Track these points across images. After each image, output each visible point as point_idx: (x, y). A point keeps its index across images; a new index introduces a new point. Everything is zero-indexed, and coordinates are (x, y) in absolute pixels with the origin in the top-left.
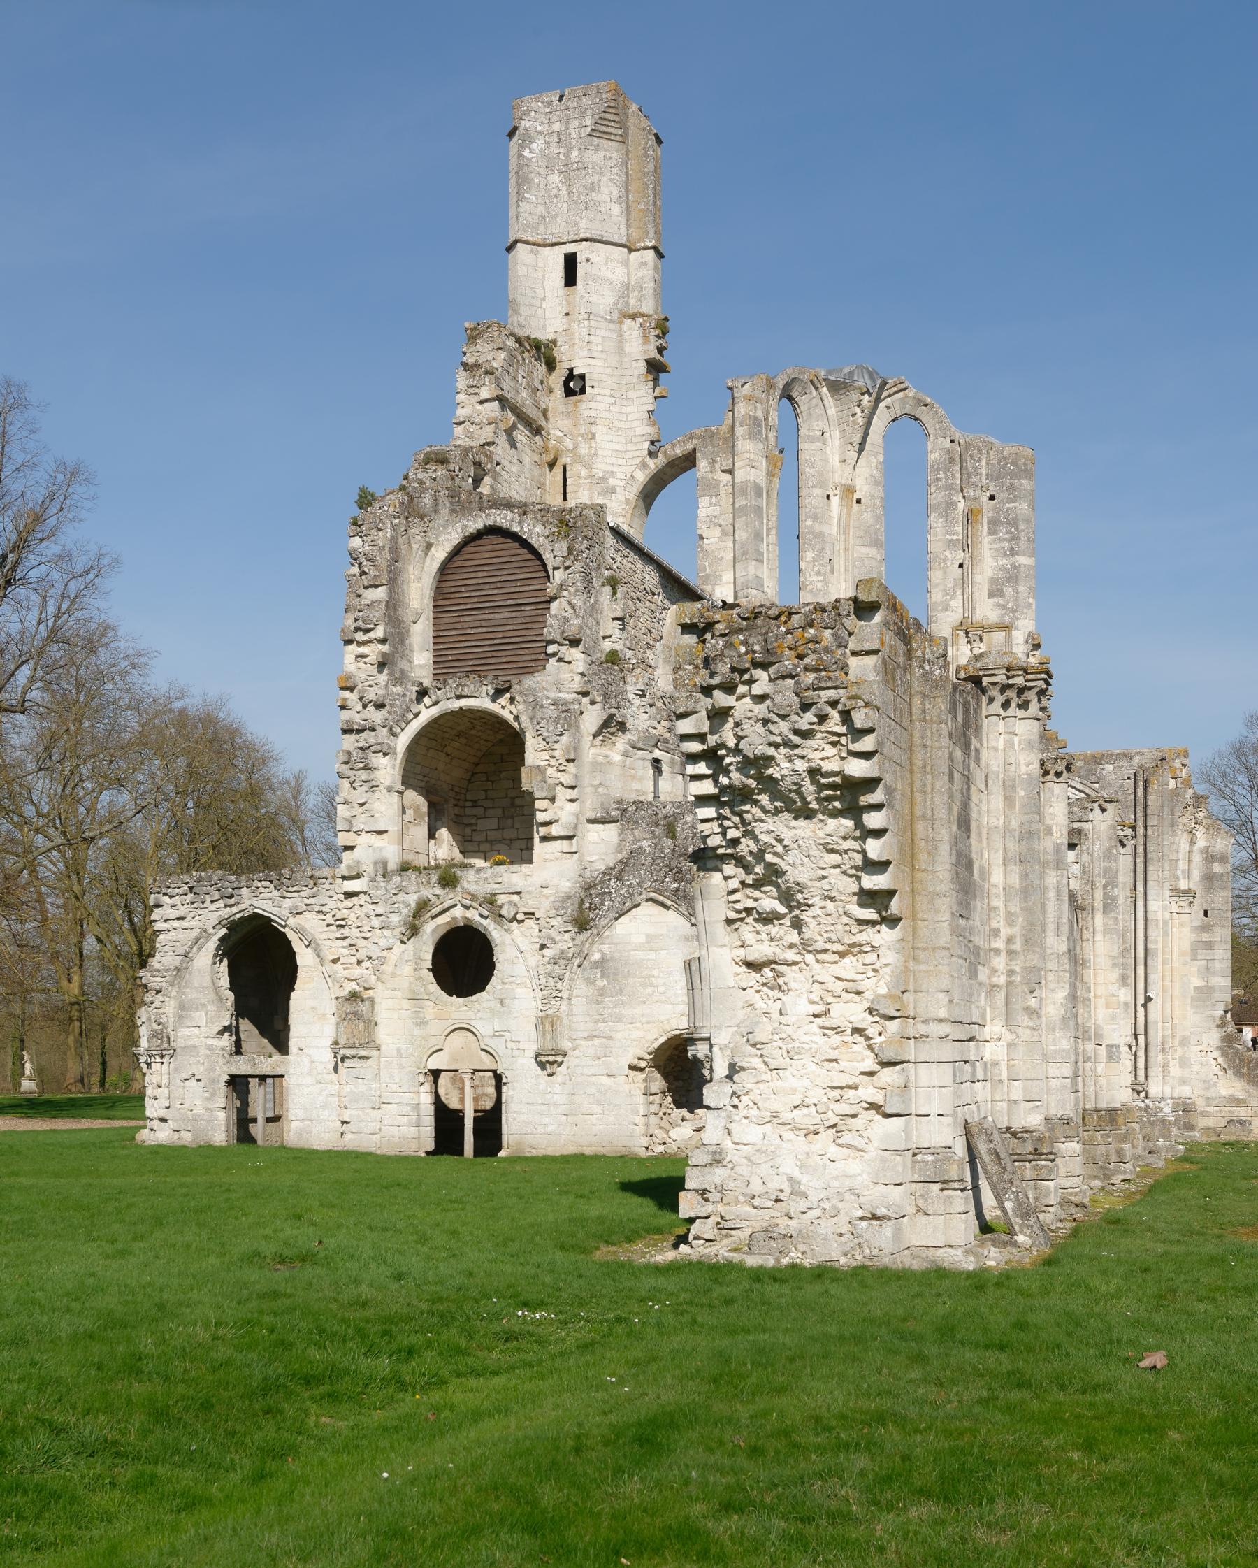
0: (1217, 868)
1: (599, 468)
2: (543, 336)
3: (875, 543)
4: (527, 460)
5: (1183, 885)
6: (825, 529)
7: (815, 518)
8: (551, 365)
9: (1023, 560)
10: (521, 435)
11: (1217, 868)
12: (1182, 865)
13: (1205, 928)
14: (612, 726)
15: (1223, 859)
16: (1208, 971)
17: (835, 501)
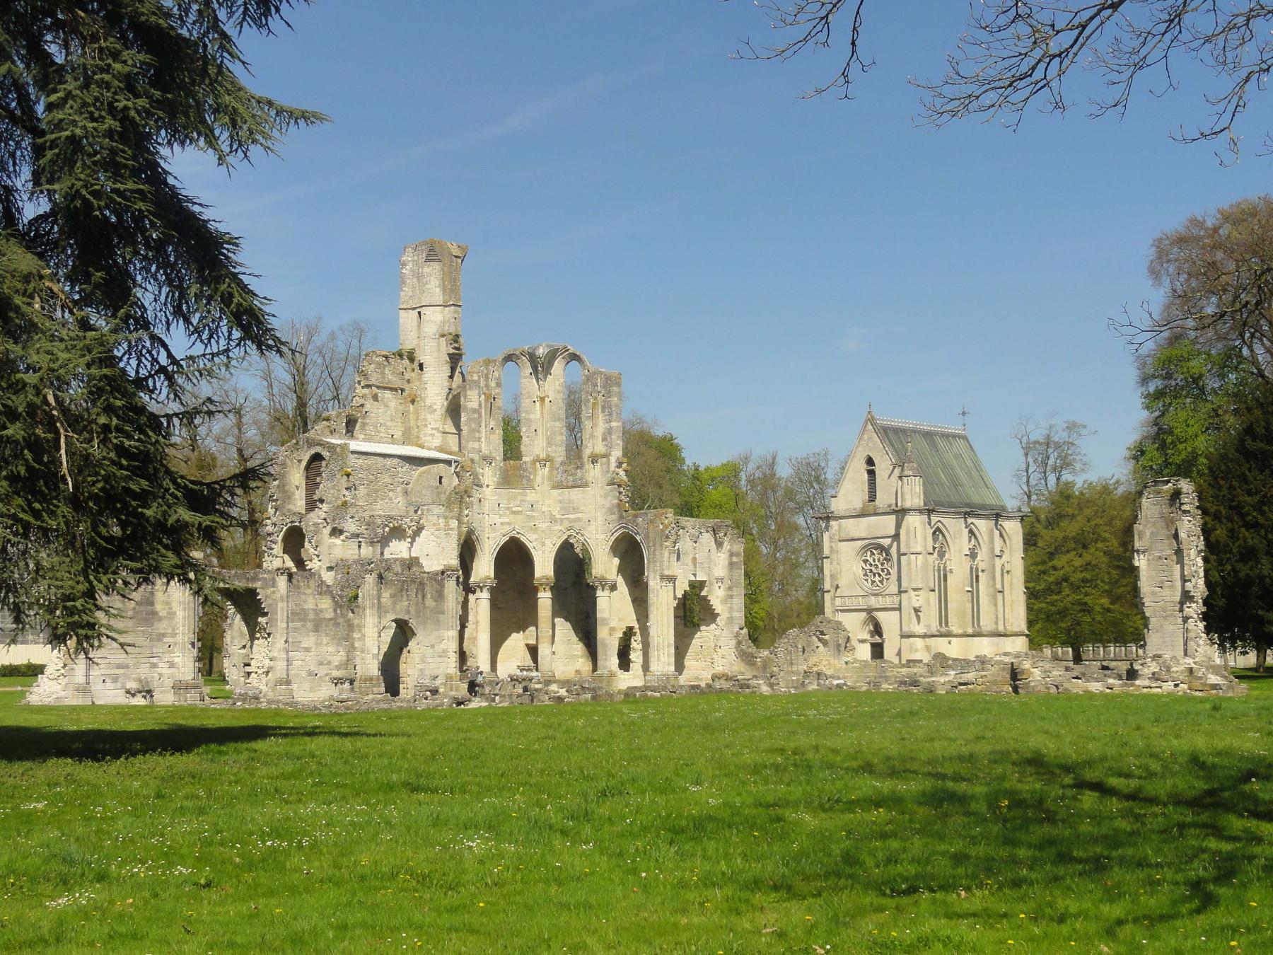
0: (734, 559)
1: (428, 402)
2: (407, 346)
3: (559, 419)
4: (392, 404)
5: (667, 573)
6: (532, 416)
7: (527, 412)
8: (412, 359)
9: (614, 424)
10: (388, 394)
11: (734, 559)
12: (666, 563)
13: (730, 588)
14: (336, 532)
15: (738, 555)
16: (731, 609)
17: (538, 404)
